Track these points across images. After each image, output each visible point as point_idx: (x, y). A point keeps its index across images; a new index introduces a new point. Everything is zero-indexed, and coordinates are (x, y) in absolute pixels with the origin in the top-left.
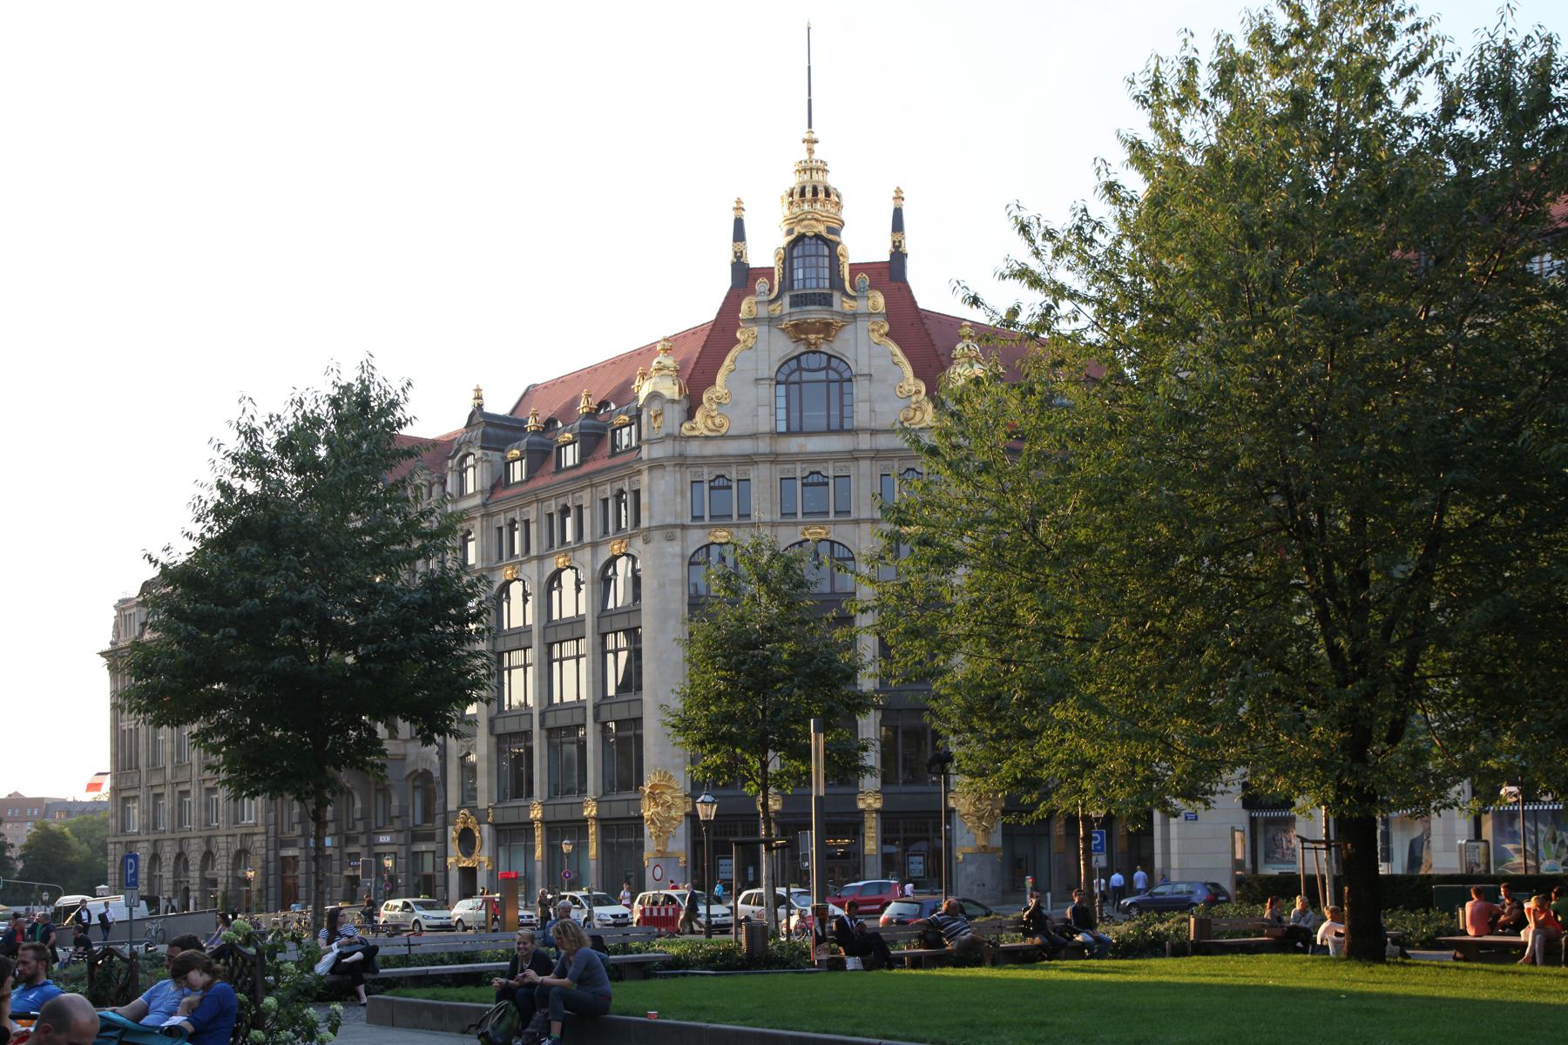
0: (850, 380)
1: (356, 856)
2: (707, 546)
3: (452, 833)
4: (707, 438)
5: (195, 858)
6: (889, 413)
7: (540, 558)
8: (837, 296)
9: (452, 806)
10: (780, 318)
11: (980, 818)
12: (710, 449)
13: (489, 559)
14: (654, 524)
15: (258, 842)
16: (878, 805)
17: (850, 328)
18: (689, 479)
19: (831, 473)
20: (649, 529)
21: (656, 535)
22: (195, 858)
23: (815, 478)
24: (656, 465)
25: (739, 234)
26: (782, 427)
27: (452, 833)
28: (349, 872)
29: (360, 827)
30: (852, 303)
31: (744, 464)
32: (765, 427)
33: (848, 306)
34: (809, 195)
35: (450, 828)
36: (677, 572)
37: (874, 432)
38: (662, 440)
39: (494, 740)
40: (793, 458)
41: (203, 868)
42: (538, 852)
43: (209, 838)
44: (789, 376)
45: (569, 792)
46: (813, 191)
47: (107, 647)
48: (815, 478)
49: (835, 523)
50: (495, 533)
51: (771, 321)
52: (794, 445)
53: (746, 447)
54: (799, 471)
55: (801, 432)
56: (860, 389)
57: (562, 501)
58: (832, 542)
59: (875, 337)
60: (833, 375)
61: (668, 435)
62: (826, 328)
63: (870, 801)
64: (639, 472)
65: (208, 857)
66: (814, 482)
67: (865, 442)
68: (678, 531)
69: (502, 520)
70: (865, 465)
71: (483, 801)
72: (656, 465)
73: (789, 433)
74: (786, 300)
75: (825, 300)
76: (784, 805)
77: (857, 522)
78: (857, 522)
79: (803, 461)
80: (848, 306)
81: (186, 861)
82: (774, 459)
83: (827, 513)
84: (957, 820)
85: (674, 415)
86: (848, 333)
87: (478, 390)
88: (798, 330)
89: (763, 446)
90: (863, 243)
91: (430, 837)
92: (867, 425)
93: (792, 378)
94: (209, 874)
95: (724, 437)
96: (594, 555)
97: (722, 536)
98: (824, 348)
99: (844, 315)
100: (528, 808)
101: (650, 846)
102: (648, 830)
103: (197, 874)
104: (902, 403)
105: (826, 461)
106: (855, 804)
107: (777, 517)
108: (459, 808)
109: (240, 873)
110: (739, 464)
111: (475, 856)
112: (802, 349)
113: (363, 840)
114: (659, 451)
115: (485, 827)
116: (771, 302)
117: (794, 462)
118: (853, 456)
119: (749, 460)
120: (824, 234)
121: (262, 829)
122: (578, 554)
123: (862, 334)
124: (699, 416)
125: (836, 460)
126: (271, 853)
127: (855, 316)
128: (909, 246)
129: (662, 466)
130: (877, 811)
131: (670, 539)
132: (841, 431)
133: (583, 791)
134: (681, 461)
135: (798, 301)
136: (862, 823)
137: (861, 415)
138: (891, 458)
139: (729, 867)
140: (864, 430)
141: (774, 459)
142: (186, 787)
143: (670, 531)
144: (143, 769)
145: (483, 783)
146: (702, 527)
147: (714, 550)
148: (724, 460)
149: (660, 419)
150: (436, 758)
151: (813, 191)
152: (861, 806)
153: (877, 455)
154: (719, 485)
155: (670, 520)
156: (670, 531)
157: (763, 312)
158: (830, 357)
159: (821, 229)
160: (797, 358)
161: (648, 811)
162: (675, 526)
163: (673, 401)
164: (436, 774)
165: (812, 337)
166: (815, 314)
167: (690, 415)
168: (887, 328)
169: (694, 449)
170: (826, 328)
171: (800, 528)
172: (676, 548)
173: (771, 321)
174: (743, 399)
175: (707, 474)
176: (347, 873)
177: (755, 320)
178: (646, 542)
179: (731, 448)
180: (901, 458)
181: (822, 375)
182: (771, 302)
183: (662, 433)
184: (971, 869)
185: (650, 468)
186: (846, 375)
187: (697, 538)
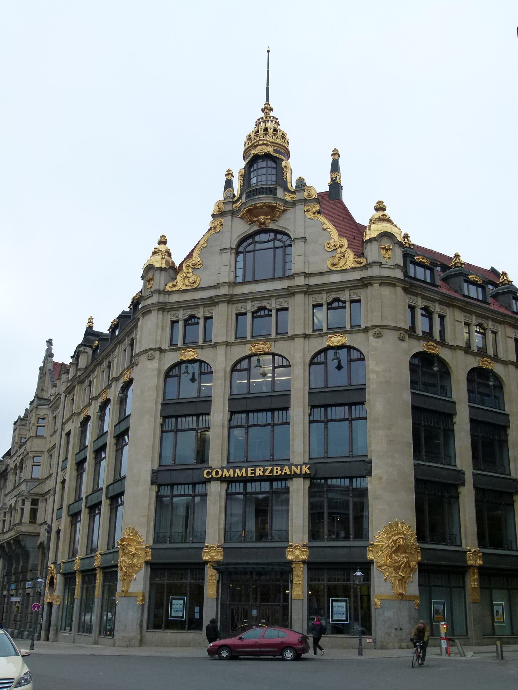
6: (320, 262)
11: (397, 569)
26: (240, 280)
30: (292, 196)
31: (209, 305)
40: (244, 299)
56: (297, 249)
58: (274, 355)
59: (310, 215)
60: (278, 244)
62: (271, 210)
63: (298, 553)
70: (299, 298)
77: (292, 338)
78: (292, 338)
84: (375, 572)
86: (290, 214)
90: (306, 168)
93: (248, 249)
98: (272, 226)
99: (285, 202)
118: (290, 293)
120: (272, 152)
125: (277, 297)
128: (344, 181)
136: (290, 571)
138: (320, 292)
141: (231, 300)
148: (195, 304)
153: (308, 290)
158: (277, 232)
159: (270, 150)
165: (261, 217)
170: (271, 210)
172: (154, 364)
175: (181, 315)
181: (271, 245)
184: (389, 614)
186: (288, 243)
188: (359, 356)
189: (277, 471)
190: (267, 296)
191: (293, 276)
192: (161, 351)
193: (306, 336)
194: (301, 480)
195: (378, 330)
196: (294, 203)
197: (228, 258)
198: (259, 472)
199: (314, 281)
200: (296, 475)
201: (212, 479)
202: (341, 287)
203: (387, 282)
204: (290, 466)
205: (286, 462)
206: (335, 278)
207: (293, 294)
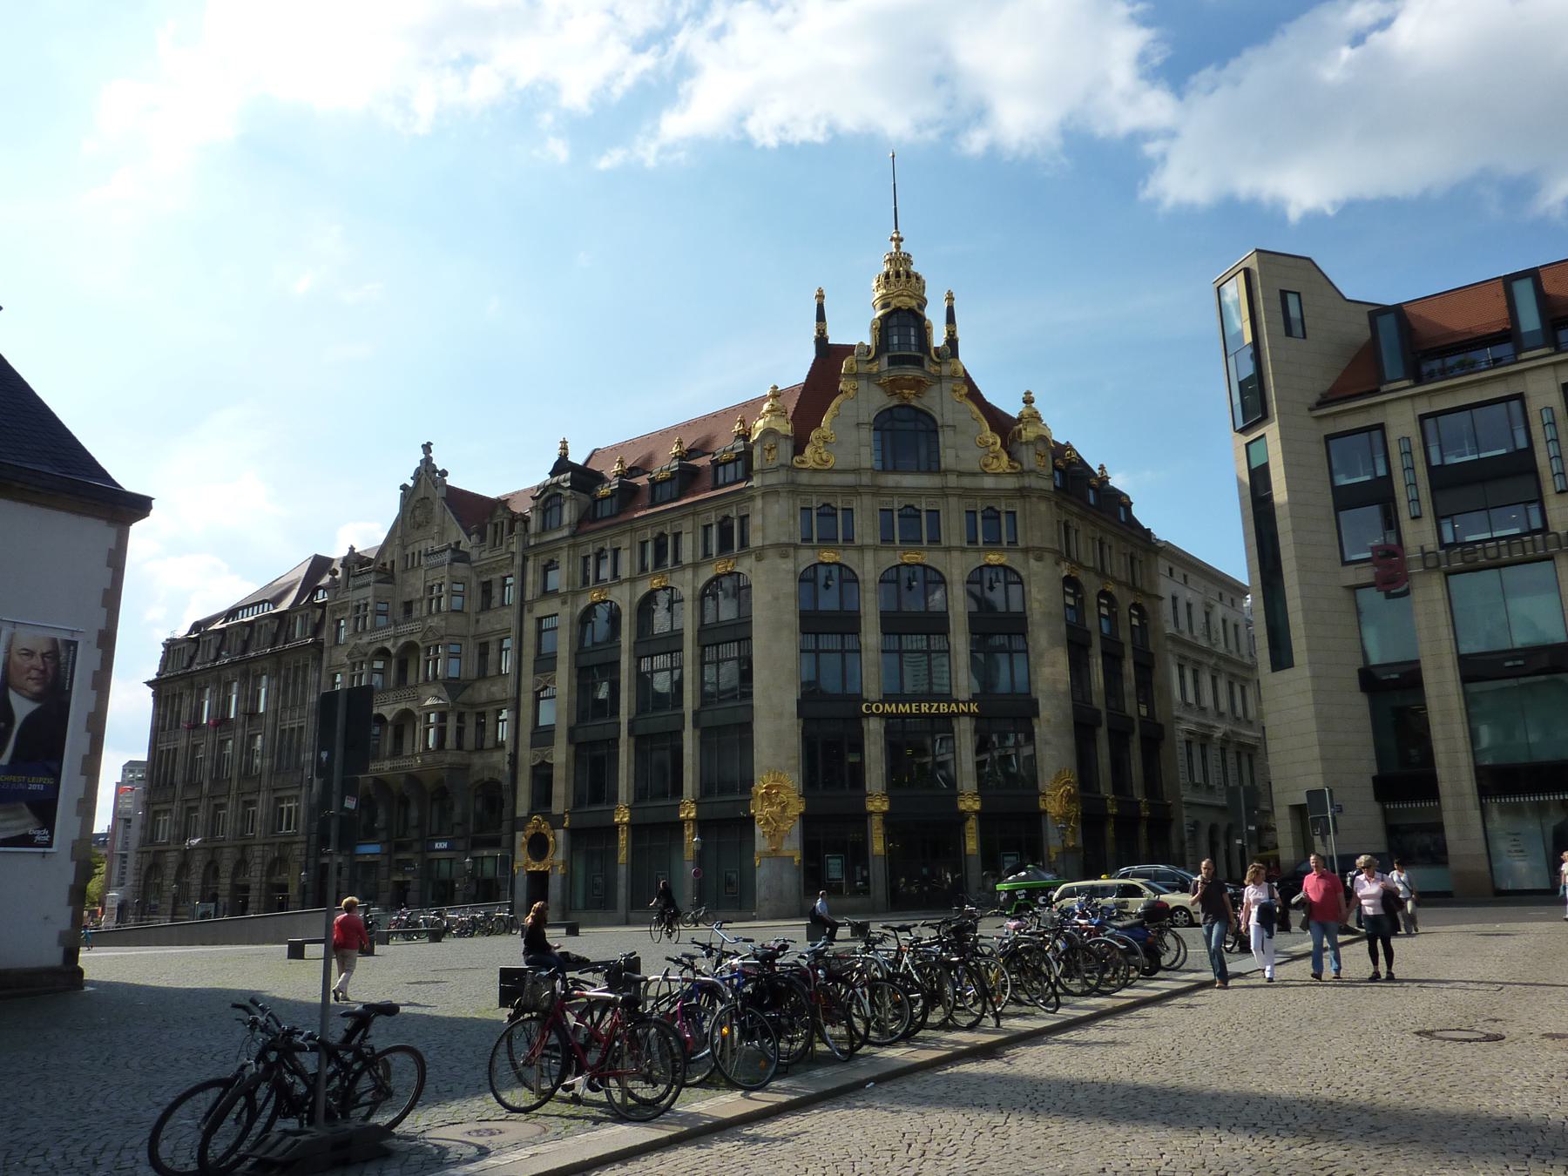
0: (936, 432)
1: (408, 862)
2: (815, 566)
3: (521, 838)
4: (815, 470)
5: (227, 863)
7: (632, 580)
8: (926, 360)
9: (522, 812)
10: (879, 374)
12: (818, 479)
13: (574, 584)
14: (767, 542)
15: (298, 850)
16: (977, 807)
17: (936, 387)
18: (799, 505)
19: (924, 506)
20: (763, 547)
21: (770, 553)
22: (227, 863)
23: (909, 511)
24: (769, 492)
25: (821, 317)
27: (521, 838)
28: (398, 878)
29: (414, 834)
31: (851, 494)
32: (867, 464)
33: (933, 369)
34: (892, 279)
35: (519, 834)
36: (790, 586)
37: (960, 474)
38: (776, 470)
39: (573, 748)
41: (235, 874)
42: (623, 856)
43: (245, 846)
44: (885, 424)
45: (664, 795)
46: (901, 275)
47: (153, 677)
48: (909, 511)
49: (929, 550)
50: (580, 562)
51: (870, 377)
52: (891, 480)
53: (850, 479)
54: (897, 504)
55: (895, 470)
56: (945, 438)
57: (658, 530)
60: (921, 426)
61: (782, 465)
62: (918, 385)
64: (752, 498)
65: (242, 865)
66: (910, 515)
67: (952, 481)
68: (791, 550)
69: (591, 550)
70: (953, 501)
71: (558, 806)
72: (769, 492)
73: (884, 470)
74: (885, 360)
75: (918, 362)
76: (891, 806)
77: (949, 549)
78: (949, 549)
79: (901, 495)
80: (933, 369)
81: (217, 870)
82: (877, 491)
83: (920, 541)
85: (786, 448)
86: (934, 391)
87: (564, 442)
88: (893, 387)
89: (865, 479)
91: (495, 843)
92: (953, 467)
94: (240, 881)
95: (831, 471)
96: (695, 575)
97: (828, 556)
98: (914, 403)
100: (612, 813)
101: (762, 844)
102: (758, 831)
103: (228, 881)
104: (980, 452)
105: (920, 496)
106: (956, 805)
107: (878, 542)
108: (531, 815)
109: (274, 880)
110: (844, 494)
111: (548, 860)
112: (895, 402)
113: (417, 847)
114: (772, 479)
115: (560, 833)
116: (870, 362)
117: (892, 495)
118: (943, 493)
119: (854, 491)
121: (304, 838)
122: (677, 576)
123: (946, 393)
124: (808, 451)
126: (311, 861)
127: (939, 378)
128: (960, 334)
129: (777, 493)
130: (976, 812)
131: (785, 556)
132: (929, 471)
133: (678, 790)
134: (794, 489)
135: (893, 361)
137: (948, 459)
139: (835, 868)
140: (952, 471)
141: (877, 491)
142: (223, 800)
143: (784, 549)
144: (179, 786)
145: (560, 790)
146: (813, 548)
147: (822, 572)
148: (833, 490)
149: (774, 452)
150: (507, 768)
151: (901, 275)
152: (962, 806)
153: (964, 493)
154: (827, 512)
155: (784, 539)
156: (784, 549)
157: (864, 368)
160: (890, 410)
161: (760, 810)
162: (788, 545)
163: (786, 437)
164: (506, 782)
166: (911, 372)
167: (798, 450)
168: (966, 389)
169: (804, 478)
171: (899, 553)
173: (870, 377)
174: (844, 439)
175: (815, 502)
176: (396, 878)
177: (857, 376)
178: (759, 559)
179: (836, 479)
180: (983, 498)
181: (911, 426)
182: (870, 362)
183: (776, 464)
185: (764, 495)
187: (807, 558)
188: (1016, 579)
189: (944, 708)
190: (919, 492)
191: (946, 472)
192: (796, 547)
193: (963, 550)
194: (967, 719)
195: (1039, 553)
196: (939, 378)
197: (867, 435)
198: (925, 708)
199: (967, 482)
200: (964, 714)
201: (873, 714)
202: (997, 493)
203: (1043, 495)
204: (957, 702)
205: (948, 698)
206: (988, 482)
207: (947, 496)
